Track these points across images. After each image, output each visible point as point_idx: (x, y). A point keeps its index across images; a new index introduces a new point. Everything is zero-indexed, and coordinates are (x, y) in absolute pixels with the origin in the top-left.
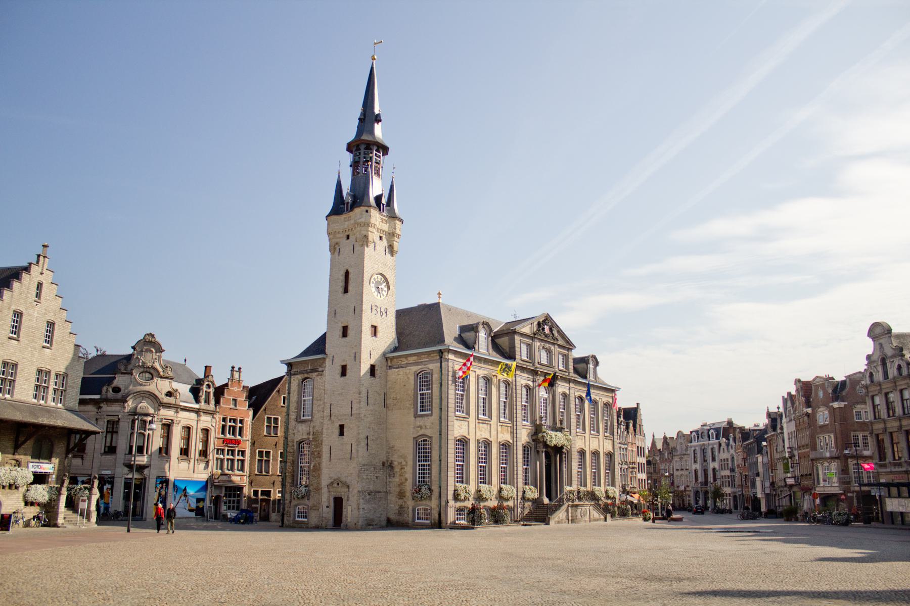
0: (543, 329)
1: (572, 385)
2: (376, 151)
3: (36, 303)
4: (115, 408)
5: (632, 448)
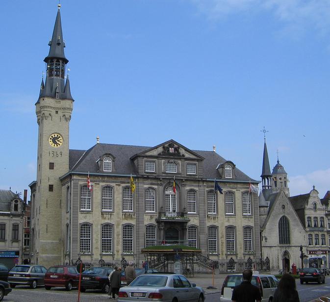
1: (201, 184)
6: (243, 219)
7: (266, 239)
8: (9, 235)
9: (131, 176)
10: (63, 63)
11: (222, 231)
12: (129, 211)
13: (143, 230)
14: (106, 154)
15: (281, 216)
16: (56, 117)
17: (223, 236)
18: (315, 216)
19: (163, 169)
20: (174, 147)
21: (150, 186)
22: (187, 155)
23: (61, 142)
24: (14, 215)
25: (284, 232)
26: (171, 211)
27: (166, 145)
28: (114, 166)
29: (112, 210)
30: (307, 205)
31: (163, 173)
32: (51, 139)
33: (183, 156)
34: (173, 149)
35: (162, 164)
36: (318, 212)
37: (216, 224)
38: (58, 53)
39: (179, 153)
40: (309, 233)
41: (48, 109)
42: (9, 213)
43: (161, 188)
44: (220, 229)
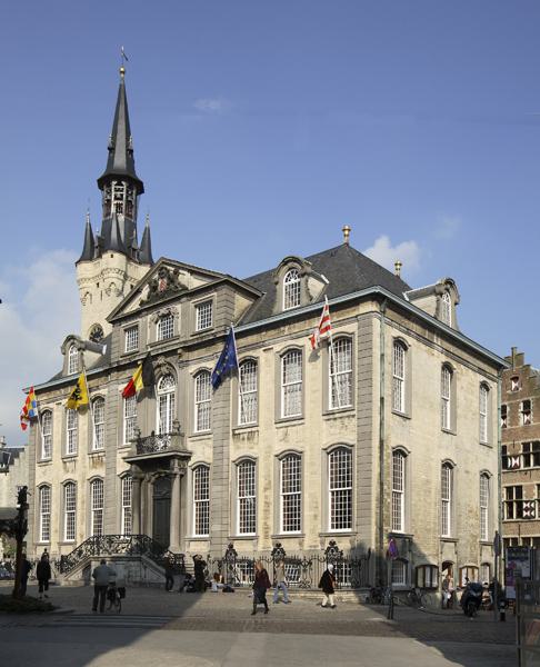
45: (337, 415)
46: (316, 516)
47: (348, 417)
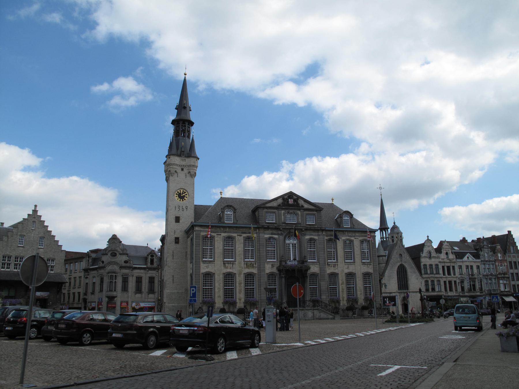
0: (288, 202)
1: (320, 233)
2: (182, 123)
3: (32, 230)
4: (102, 271)
5: (501, 263)
6: (362, 266)
7: (385, 286)
8: (145, 288)
9: (252, 226)
10: (188, 124)
11: (342, 278)
12: (251, 260)
13: (265, 279)
14: (228, 206)
15: (399, 264)
16: (182, 174)
17: (343, 282)
18: (430, 263)
19: (283, 220)
20: (293, 199)
21: (270, 236)
22: (306, 206)
23: (186, 197)
24: (150, 269)
25: (402, 279)
26: (292, 259)
27: (286, 197)
28: (235, 217)
29: (233, 260)
30: (422, 253)
31: (283, 223)
32: (177, 194)
33: (302, 206)
34: (292, 200)
35: (282, 215)
36: (433, 260)
37: (336, 271)
38: (183, 117)
39: (298, 204)
40: (425, 279)
41: (175, 167)
42: (145, 266)
43: (282, 237)
44: (340, 276)
45: (366, 264)
46: (361, 294)
47: (369, 264)
